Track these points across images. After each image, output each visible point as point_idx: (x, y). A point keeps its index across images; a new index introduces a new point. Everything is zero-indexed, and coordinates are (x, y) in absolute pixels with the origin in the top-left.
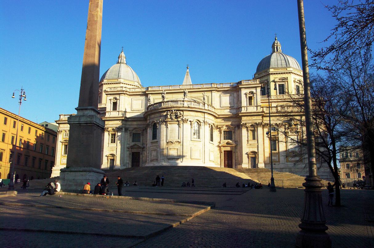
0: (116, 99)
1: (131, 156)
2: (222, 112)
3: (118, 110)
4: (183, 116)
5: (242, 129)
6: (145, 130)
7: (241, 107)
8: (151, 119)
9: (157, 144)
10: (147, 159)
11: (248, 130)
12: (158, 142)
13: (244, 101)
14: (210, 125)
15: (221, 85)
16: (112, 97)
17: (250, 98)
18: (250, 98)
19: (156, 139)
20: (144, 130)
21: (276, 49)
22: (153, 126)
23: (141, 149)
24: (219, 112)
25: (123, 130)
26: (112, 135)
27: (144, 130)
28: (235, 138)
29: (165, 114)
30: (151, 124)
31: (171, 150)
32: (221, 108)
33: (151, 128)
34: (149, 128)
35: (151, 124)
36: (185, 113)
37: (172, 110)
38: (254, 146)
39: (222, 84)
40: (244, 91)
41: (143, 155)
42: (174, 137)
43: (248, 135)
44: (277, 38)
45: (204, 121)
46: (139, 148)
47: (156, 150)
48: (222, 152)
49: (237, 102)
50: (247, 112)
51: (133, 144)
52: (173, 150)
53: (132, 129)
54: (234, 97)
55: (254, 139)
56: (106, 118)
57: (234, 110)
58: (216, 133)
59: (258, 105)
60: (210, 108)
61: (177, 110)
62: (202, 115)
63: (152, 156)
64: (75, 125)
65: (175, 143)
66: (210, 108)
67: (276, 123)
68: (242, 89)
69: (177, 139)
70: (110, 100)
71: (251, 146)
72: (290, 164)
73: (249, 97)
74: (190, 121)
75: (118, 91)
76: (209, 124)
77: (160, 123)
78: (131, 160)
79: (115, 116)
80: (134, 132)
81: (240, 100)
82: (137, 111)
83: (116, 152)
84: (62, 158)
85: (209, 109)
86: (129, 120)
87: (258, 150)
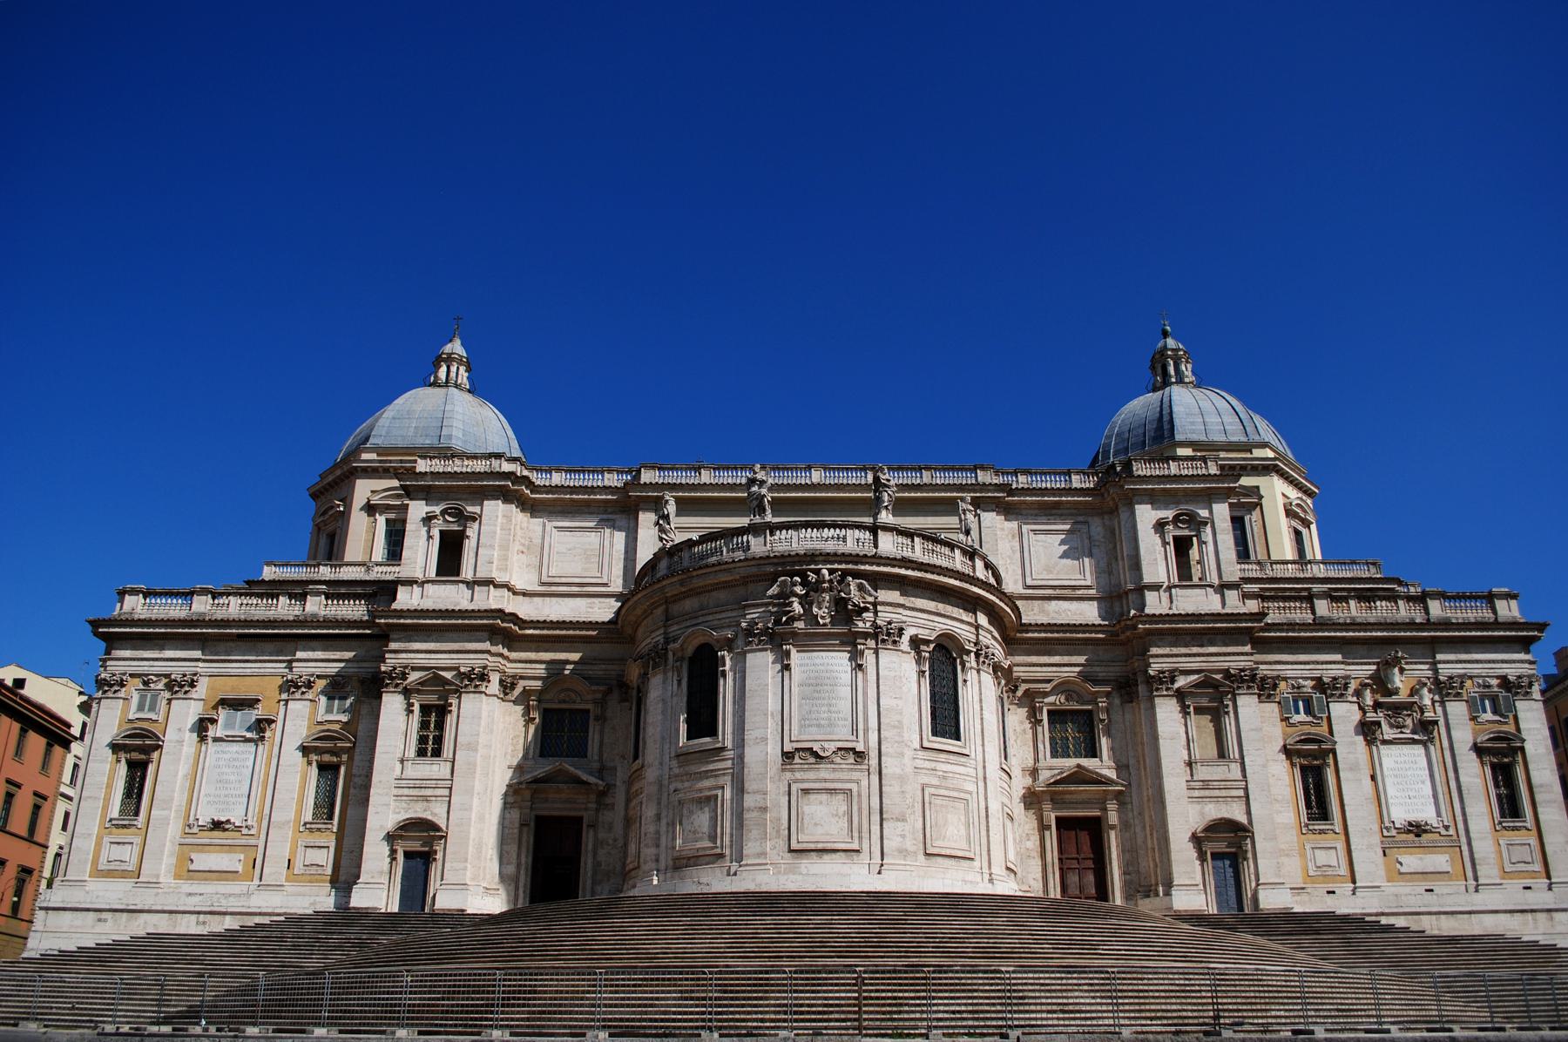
1: (529, 838)
2: (1036, 610)
3: (467, 572)
4: (875, 604)
5: (1157, 701)
7: (1141, 589)
10: (648, 852)
11: (1185, 711)
13: (1156, 562)
15: (1022, 478)
17: (1182, 546)
18: (1182, 546)
20: (610, 691)
21: (1171, 370)
22: (692, 660)
25: (494, 686)
26: (425, 710)
29: (774, 590)
31: (812, 797)
38: (1224, 793)
39: (1027, 472)
40: (1146, 516)
41: (601, 835)
42: (822, 722)
43: (1187, 733)
44: (1168, 328)
45: (976, 644)
48: (1049, 827)
49: (1109, 564)
50: (1171, 612)
51: (545, 767)
52: (824, 797)
54: (1090, 538)
55: (1222, 754)
58: (1017, 718)
59: (1227, 578)
61: (845, 573)
65: (838, 760)
67: (1317, 674)
69: (842, 734)
71: (1207, 793)
72: (1407, 890)
73: (1175, 538)
74: (916, 642)
77: (740, 642)
83: (448, 812)
84: (106, 840)
87: (1249, 813)
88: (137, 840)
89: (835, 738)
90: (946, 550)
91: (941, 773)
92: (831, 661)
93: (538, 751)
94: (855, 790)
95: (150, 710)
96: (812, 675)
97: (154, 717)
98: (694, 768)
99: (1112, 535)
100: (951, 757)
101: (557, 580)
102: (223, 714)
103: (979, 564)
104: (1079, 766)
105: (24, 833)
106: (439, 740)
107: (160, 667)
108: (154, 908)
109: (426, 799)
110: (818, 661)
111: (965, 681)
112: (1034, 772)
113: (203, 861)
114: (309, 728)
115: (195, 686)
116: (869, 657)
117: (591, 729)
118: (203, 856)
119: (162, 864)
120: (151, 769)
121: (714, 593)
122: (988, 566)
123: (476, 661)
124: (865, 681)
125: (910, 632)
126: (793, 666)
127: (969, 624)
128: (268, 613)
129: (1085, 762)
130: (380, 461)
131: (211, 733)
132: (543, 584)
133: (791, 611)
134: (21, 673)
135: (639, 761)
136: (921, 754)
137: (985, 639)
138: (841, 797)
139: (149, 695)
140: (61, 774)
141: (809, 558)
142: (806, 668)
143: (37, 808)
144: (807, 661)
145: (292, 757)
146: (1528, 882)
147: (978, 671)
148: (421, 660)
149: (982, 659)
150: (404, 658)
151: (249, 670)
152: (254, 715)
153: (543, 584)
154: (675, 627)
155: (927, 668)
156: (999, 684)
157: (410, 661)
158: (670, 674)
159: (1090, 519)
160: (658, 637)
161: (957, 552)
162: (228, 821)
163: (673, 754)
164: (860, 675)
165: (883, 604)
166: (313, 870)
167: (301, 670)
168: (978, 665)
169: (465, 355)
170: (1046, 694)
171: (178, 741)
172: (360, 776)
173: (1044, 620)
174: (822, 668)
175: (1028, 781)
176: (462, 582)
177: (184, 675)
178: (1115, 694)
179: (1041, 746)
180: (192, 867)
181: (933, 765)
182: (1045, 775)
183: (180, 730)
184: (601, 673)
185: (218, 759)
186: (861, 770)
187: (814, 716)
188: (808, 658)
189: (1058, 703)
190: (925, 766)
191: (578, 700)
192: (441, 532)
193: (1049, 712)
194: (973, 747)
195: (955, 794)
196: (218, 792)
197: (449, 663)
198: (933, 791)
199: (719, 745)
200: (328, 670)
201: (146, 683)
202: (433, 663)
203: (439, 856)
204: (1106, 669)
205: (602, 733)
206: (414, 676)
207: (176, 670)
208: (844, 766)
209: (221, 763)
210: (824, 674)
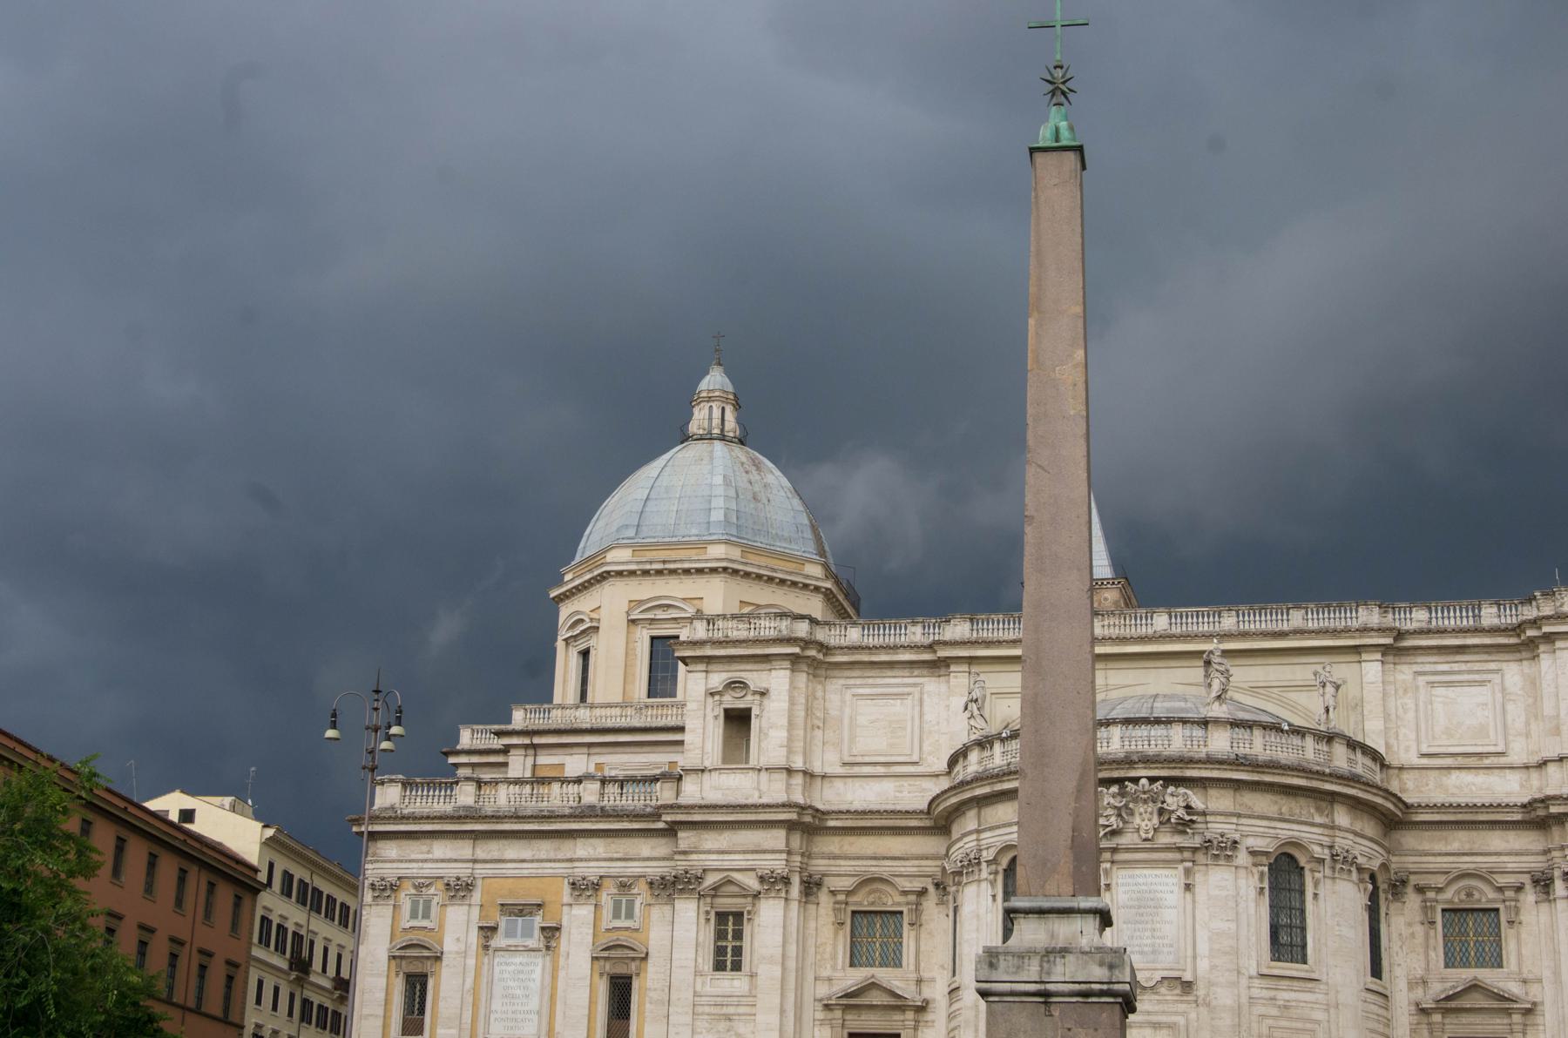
2: (1432, 785)
6: (931, 889)
8: (991, 829)
14: (1366, 877)
16: (718, 679)
20: (923, 893)
22: (1005, 870)
23: (910, 1015)
24: (1410, 785)
25: (795, 889)
26: (722, 917)
27: (923, 893)
28: (1519, 955)
30: (989, 862)
32: (1425, 762)
33: (993, 883)
34: (979, 881)
35: (994, 861)
36: (1220, 801)
37: (1136, 780)
42: (1146, 949)
45: (1331, 847)
49: (1527, 724)
51: (856, 977)
53: (847, 883)
54: (1503, 690)
56: (689, 808)
57: (1509, 774)
60: (1362, 765)
61: (1168, 781)
62: (1318, 809)
64: (1017, 999)
66: (1362, 765)
70: (712, 694)
74: (1253, 853)
75: (757, 642)
76: (1360, 870)
79: (743, 801)
80: (860, 904)
81: (1548, 708)
82: (881, 770)
85: (1359, 770)
86: (831, 823)
89: (1159, 966)
90: (1296, 740)
91: (1281, 1003)
92: (1154, 880)
93: (848, 961)
94: (1181, 1020)
95: (423, 917)
96: (1134, 896)
99: (1533, 684)
100: (1295, 983)
102: (503, 923)
103: (1340, 750)
104: (1475, 978)
105: (218, 1012)
106: (738, 951)
107: (429, 870)
109: (728, 1018)
110: (1141, 880)
111: (1316, 895)
112: (1425, 982)
114: (594, 935)
115: (471, 890)
116: (1199, 878)
117: (905, 935)
120: (431, 983)
122: (1353, 745)
123: (777, 864)
124: (1194, 901)
125: (1250, 842)
126: (1113, 886)
127: (1320, 825)
128: (540, 804)
129: (1486, 975)
130: (638, 563)
131: (494, 943)
132: (845, 764)
133: (1108, 826)
134: (188, 802)
135: (956, 978)
136: (1257, 982)
137: (1343, 842)
138: (1164, 1032)
139: (421, 902)
140: (251, 934)
141: (1127, 766)
142: (1127, 888)
143: (230, 978)
144: (1129, 880)
147: (1334, 878)
148: (712, 861)
149: (1339, 866)
150: (697, 861)
151: (526, 871)
152: (538, 921)
153: (845, 764)
155: (1266, 885)
156: (1365, 889)
157: (701, 863)
158: (984, 885)
159: (1504, 666)
160: (969, 844)
161: (1309, 741)
164: (1188, 895)
165: (1213, 814)
167: (581, 870)
168: (1334, 871)
169: (730, 388)
170: (1439, 890)
171: (457, 953)
172: (655, 990)
173: (1439, 798)
174: (1144, 888)
175: (1419, 993)
176: (752, 769)
177: (458, 879)
178: (1529, 887)
179: (1432, 954)
181: (1272, 993)
182: (1437, 989)
183: (458, 939)
184: (915, 869)
185: (501, 972)
186: (1188, 1002)
187: (1136, 942)
188: (1130, 877)
189: (1456, 900)
190: (1260, 995)
191: (890, 902)
192: (726, 710)
193: (1444, 910)
194: (1324, 969)
195: (1299, 1025)
196: (505, 1008)
197: (743, 864)
198: (1270, 1022)
200: (612, 870)
201: (418, 887)
202: (726, 865)
204: (1513, 859)
205: (918, 940)
206: (711, 880)
207: (452, 871)
208: (1169, 998)
209: (506, 976)
210: (1147, 895)
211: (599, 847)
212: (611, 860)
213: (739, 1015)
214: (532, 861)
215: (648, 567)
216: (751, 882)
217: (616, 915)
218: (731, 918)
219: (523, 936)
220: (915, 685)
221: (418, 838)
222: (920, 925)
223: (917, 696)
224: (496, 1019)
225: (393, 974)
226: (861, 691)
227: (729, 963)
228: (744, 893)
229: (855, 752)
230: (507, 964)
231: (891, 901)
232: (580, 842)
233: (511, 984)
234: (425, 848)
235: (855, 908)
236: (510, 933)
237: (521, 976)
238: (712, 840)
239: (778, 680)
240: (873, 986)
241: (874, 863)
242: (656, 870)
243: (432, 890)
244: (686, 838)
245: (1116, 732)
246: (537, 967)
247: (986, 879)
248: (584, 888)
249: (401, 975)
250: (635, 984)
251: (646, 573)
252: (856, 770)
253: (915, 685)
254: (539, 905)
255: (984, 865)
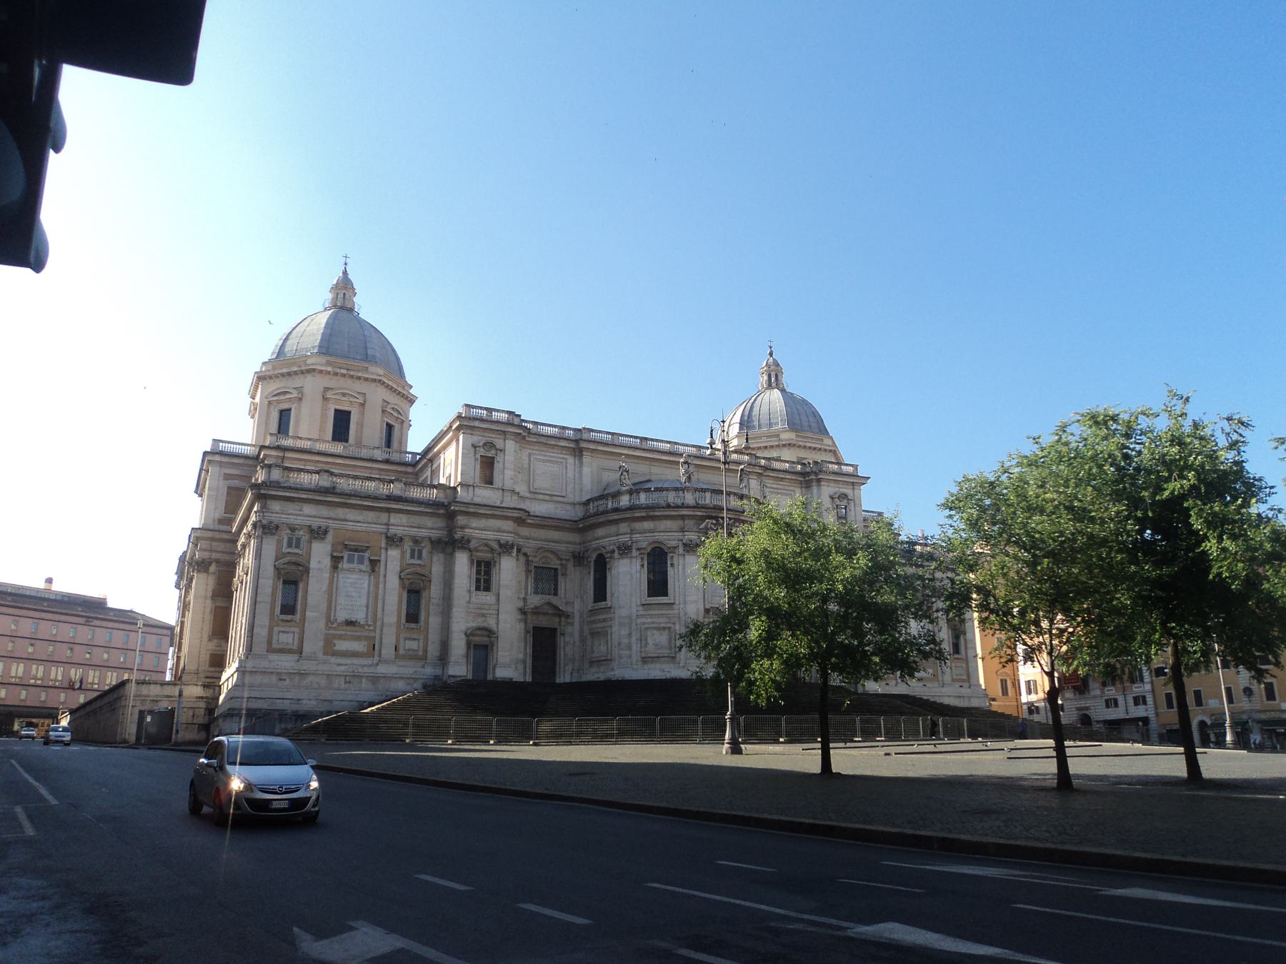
0: (489, 445)
1: (530, 639)
9: (670, 612)
12: (674, 606)
19: (665, 594)
26: (479, 563)
33: (642, 559)
34: (631, 557)
41: (567, 639)
46: (554, 615)
47: (670, 628)
51: (535, 600)
63: (651, 647)
68: (822, 483)
75: (498, 422)
78: (529, 650)
84: (276, 629)
88: (297, 630)
97: (300, 552)
98: (654, 612)
101: (538, 491)
102: (346, 554)
107: (299, 521)
108: (317, 672)
109: (484, 615)
113: (342, 645)
118: (342, 642)
119: (313, 645)
120: (301, 586)
121: (665, 522)
131: (340, 565)
135: (609, 603)
145: (393, 582)
146: (961, 684)
148: (476, 533)
152: (366, 555)
153: (530, 492)
154: (638, 535)
158: (634, 560)
162: (356, 621)
163: (639, 603)
166: (411, 653)
167: (393, 530)
171: (319, 569)
172: (435, 598)
177: (320, 527)
180: (335, 648)
183: (319, 562)
185: (344, 582)
199: (672, 601)
202: (483, 537)
203: (495, 648)
207: (316, 523)
211: (403, 519)
212: (411, 527)
213: (490, 614)
214: (363, 523)
215: (338, 371)
216: (495, 546)
217: (412, 557)
218: (483, 564)
219: (357, 563)
220: (563, 458)
221: (294, 501)
222: (566, 575)
223: (564, 463)
224: (341, 609)
225: (276, 580)
226: (538, 457)
227: (482, 587)
228: (492, 550)
229: (535, 487)
230: (348, 578)
231: (555, 563)
232: (392, 515)
233: (350, 589)
234: (298, 508)
235: (536, 565)
236: (350, 560)
237: (356, 585)
238: (475, 523)
239: (510, 445)
240: (549, 604)
241: (546, 543)
242: (435, 534)
243: (301, 533)
244: (461, 520)
245: (708, 495)
246: (364, 582)
247: (636, 557)
248: (393, 541)
249: (281, 580)
250: (424, 594)
251: (336, 374)
252: (537, 496)
253: (563, 458)
254: (368, 547)
255: (634, 551)
